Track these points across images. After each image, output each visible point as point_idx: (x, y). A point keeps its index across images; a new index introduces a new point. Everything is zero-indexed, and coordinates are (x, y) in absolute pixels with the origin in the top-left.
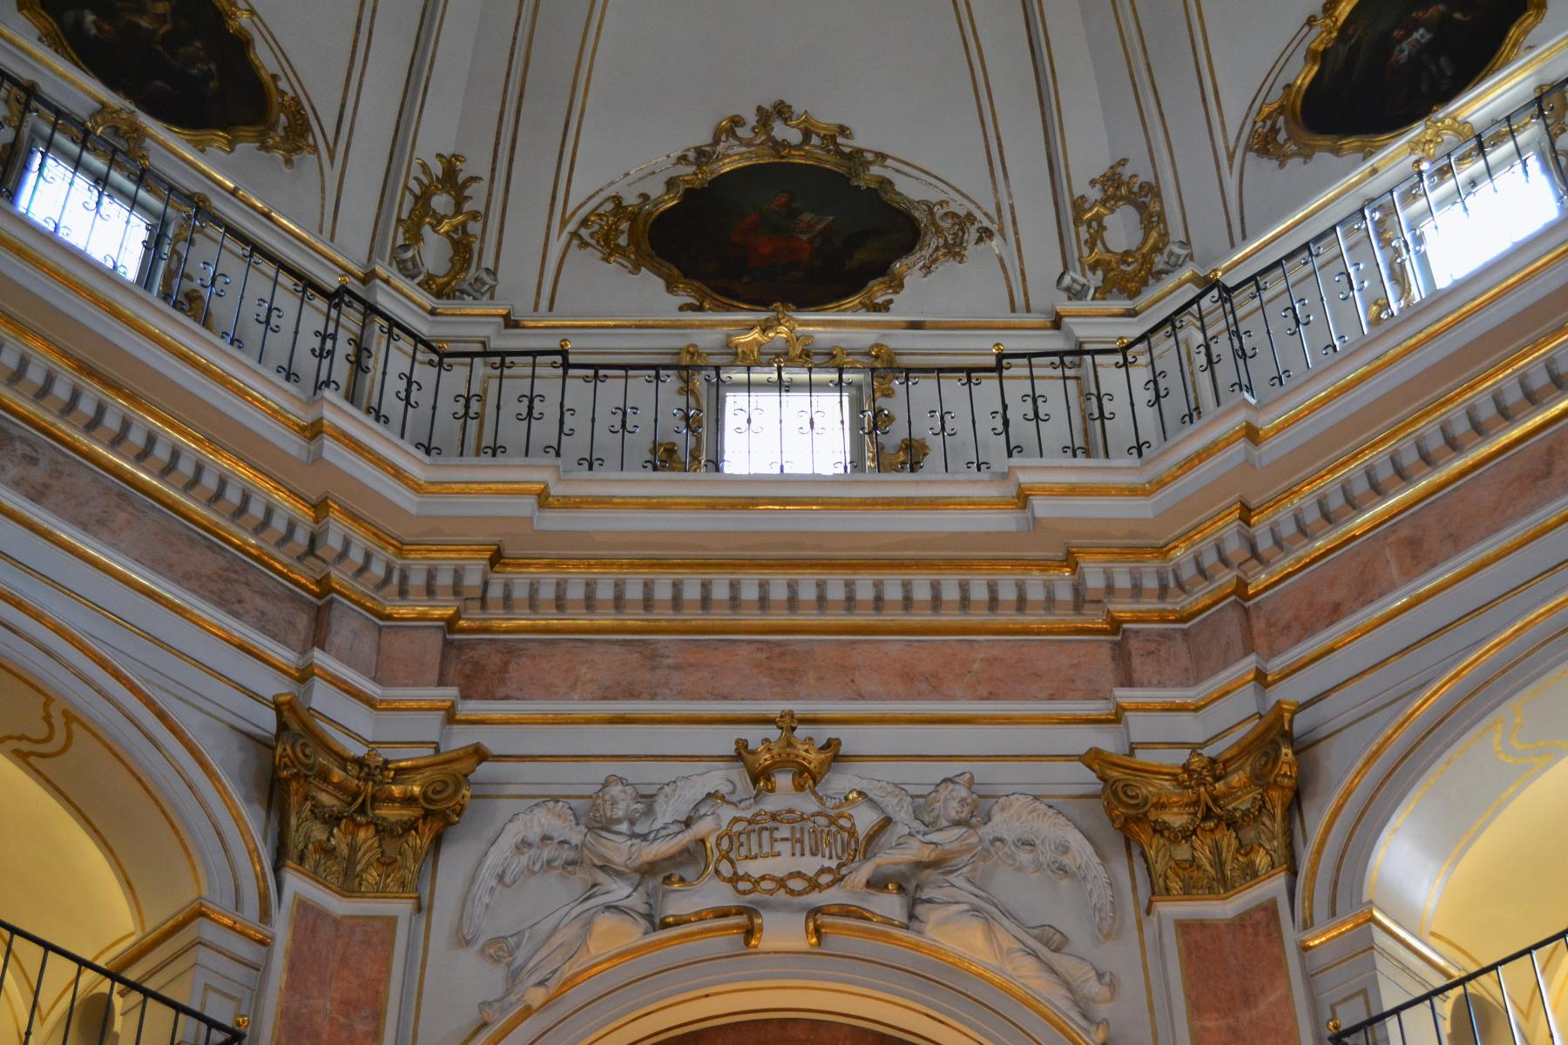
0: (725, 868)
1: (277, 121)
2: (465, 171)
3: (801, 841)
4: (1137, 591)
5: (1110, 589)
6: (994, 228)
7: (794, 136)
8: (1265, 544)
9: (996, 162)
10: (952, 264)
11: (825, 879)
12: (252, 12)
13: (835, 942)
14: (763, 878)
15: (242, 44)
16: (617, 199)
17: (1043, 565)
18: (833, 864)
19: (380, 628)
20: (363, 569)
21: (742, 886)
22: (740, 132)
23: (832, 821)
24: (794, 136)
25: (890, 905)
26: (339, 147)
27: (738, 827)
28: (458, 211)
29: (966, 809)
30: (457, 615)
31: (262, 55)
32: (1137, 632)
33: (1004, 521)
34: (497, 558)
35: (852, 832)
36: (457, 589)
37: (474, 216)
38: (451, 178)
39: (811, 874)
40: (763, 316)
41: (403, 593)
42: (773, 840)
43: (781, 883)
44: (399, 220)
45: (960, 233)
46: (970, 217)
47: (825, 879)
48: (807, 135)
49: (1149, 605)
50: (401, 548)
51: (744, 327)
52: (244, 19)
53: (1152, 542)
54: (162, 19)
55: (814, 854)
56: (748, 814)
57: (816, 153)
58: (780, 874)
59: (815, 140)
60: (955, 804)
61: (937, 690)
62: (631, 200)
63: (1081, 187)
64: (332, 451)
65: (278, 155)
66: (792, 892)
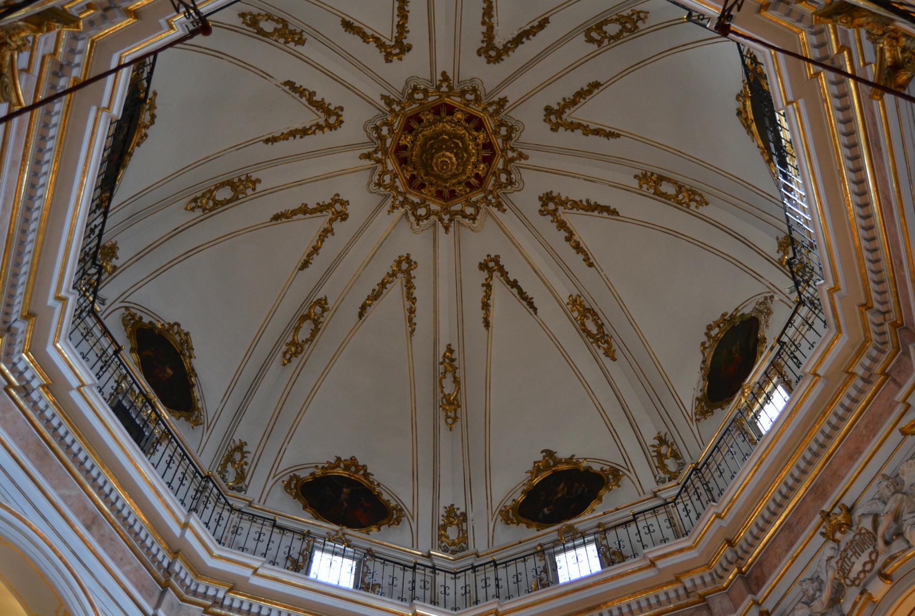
0: (848, 582)
1: (608, 479)
2: (663, 434)
3: (856, 552)
4: (874, 360)
5: (868, 369)
6: (772, 294)
7: (717, 330)
8: (882, 308)
9: (757, 276)
10: (771, 317)
11: (874, 557)
12: (585, 459)
13: (896, 576)
14: (858, 575)
15: (588, 470)
16: (697, 399)
17: (845, 384)
18: (871, 549)
19: (727, 593)
20: (704, 583)
21: (857, 582)
22: (707, 345)
23: (860, 534)
24: (717, 330)
25: (897, 546)
26: (630, 467)
27: (840, 564)
28: (669, 447)
29: (891, 488)
30: (740, 569)
31: (596, 467)
32: (891, 370)
33: (820, 386)
34: (730, 543)
35: (868, 532)
36: (731, 563)
37: (672, 444)
38: (662, 441)
39: (868, 559)
40: (740, 392)
41: (721, 577)
42: (849, 559)
43: (864, 571)
44: (657, 468)
45: (764, 307)
46: (766, 298)
47: (874, 557)
48: (719, 326)
49: (884, 358)
50: (708, 566)
51: (740, 399)
52: (585, 464)
53: (861, 342)
54: (563, 488)
55: (863, 552)
56: (839, 557)
57: (725, 327)
58: (861, 568)
59: (722, 325)
60: (886, 490)
61: (859, 451)
62: (699, 394)
63: (777, 257)
64: (660, 564)
65: (615, 488)
66: (869, 572)
